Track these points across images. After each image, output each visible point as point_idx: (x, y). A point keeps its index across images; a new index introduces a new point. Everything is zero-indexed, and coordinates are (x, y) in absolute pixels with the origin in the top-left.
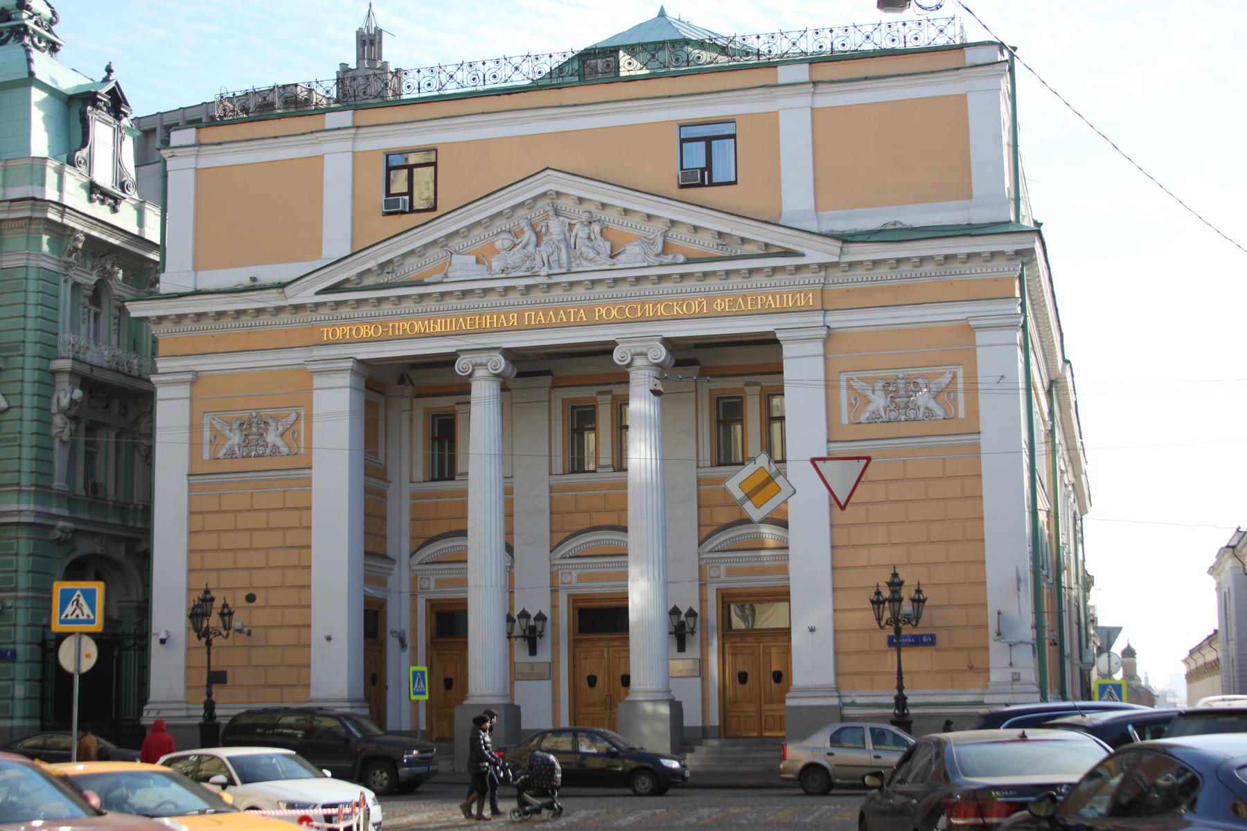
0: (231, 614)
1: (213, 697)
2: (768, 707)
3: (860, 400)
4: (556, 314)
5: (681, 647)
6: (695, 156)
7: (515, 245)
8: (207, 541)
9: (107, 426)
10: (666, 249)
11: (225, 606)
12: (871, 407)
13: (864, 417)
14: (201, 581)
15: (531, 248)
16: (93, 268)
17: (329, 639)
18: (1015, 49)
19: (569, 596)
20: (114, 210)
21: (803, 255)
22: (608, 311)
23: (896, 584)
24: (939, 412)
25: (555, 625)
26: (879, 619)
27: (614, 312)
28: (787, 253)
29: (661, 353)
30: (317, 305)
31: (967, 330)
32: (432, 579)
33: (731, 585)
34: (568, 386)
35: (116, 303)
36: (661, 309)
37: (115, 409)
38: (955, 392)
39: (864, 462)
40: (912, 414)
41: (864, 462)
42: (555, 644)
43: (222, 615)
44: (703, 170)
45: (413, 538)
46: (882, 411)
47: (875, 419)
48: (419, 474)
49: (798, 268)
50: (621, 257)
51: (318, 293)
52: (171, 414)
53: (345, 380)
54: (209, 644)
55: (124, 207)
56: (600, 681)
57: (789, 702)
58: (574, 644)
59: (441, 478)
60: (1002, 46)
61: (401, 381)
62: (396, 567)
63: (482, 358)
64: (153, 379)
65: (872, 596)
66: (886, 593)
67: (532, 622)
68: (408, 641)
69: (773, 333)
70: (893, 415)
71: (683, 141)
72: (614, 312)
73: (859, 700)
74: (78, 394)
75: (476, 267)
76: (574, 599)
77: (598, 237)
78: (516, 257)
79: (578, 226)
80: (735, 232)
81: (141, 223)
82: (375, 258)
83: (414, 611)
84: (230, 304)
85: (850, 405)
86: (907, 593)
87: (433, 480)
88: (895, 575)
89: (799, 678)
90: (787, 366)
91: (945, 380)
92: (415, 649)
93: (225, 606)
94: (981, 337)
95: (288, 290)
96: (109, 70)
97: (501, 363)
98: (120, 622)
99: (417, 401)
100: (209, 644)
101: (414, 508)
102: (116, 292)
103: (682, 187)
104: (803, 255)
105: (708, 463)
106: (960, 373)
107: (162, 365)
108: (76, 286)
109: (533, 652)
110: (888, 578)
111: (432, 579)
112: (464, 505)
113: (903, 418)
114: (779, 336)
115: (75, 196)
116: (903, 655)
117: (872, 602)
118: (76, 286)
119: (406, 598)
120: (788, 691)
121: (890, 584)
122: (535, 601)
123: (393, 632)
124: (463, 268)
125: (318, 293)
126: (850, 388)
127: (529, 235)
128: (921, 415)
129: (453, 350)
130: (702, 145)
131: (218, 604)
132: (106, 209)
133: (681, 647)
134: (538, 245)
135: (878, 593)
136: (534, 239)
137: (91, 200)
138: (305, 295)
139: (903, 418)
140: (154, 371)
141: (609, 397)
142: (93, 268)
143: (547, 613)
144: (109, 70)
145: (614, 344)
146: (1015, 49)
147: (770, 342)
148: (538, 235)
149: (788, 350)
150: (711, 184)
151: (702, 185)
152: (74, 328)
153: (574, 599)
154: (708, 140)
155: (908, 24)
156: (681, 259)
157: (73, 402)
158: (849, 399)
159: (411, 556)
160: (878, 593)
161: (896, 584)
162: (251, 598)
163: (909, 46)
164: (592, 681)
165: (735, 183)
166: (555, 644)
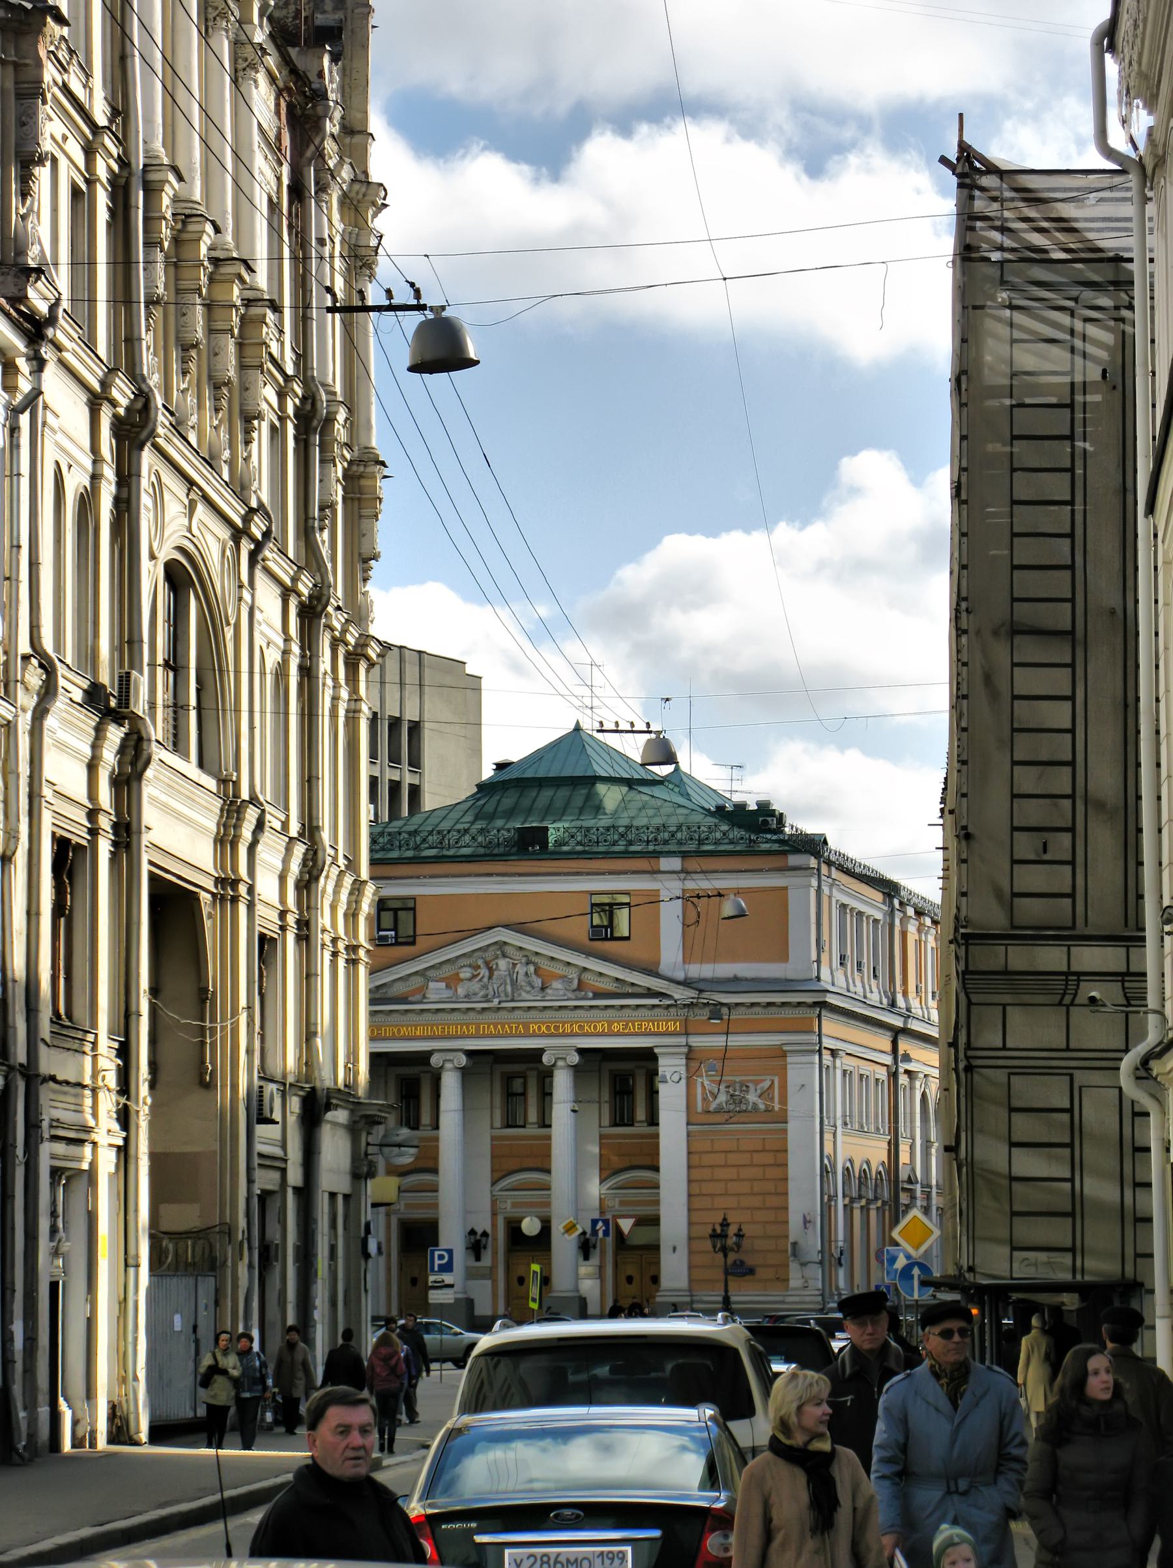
4: (503, 1028)
5: (586, 1258)
7: (474, 976)
10: (581, 986)
13: (712, 1107)
15: (486, 980)
22: (539, 1028)
23: (725, 1224)
25: (495, 1239)
26: (714, 1247)
27: (543, 1028)
29: (575, 1059)
34: (512, 1078)
36: (576, 1028)
40: (744, 1107)
42: (495, 1253)
44: (606, 927)
47: (719, 1110)
50: (549, 991)
57: (658, 1299)
63: (450, 1056)
67: (478, 1237)
69: (651, 1049)
70: (732, 1107)
72: (543, 1028)
73: (705, 1299)
78: (475, 986)
86: (732, 1230)
89: (665, 1282)
91: (767, 1084)
97: (463, 1060)
103: (591, 940)
109: (478, 1259)
114: (656, 1050)
120: (658, 1291)
121: (722, 1225)
122: (483, 1223)
127: (484, 972)
133: (586, 1258)
134: (490, 977)
135: (714, 1230)
136: (487, 973)
143: (489, 1231)
148: (491, 970)
151: (606, 939)
160: (714, 1230)
161: (725, 1224)
165: (628, 938)
166: (495, 1253)
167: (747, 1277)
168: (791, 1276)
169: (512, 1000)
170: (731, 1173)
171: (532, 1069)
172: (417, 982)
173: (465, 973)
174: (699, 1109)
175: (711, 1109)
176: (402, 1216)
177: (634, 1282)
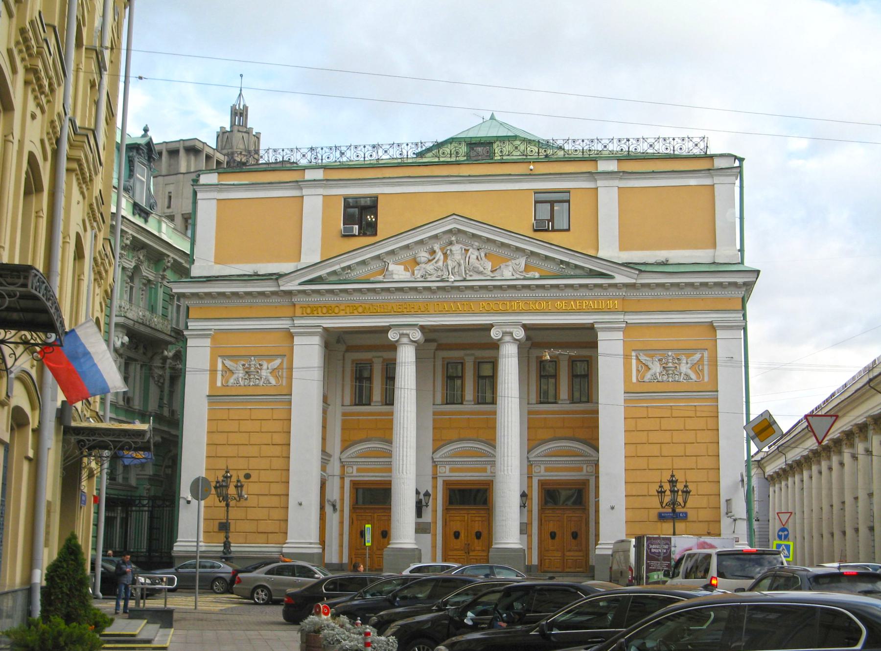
0: (242, 486)
1: (230, 540)
2: (568, 554)
6: (544, 211)
7: (430, 261)
8: (220, 438)
9: (135, 360)
11: (238, 481)
14: (222, 464)
16: (133, 257)
17: (612, 508)
18: (743, 159)
19: (444, 481)
20: (146, 221)
21: (612, 277)
24: (693, 376)
26: (661, 503)
29: (520, 334)
30: (300, 292)
31: (712, 327)
32: (355, 468)
33: (547, 478)
35: (144, 281)
37: (141, 351)
38: (703, 365)
39: (834, 418)
41: (834, 418)
42: (435, 511)
43: (236, 487)
44: (549, 221)
45: (343, 441)
48: (347, 401)
49: (610, 285)
52: (198, 355)
53: (316, 340)
54: (228, 505)
55: (151, 219)
56: (462, 535)
58: (446, 510)
59: (360, 404)
60: (736, 158)
61: (338, 341)
62: (332, 459)
64: (185, 333)
65: (657, 488)
66: (667, 487)
68: (338, 507)
69: (592, 324)
71: (536, 202)
74: (126, 339)
75: (404, 273)
77: (484, 258)
78: (430, 267)
79: (471, 250)
80: (571, 261)
81: (160, 231)
82: (339, 264)
83: (342, 488)
84: (241, 288)
85: (638, 371)
86: (680, 486)
87: (356, 405)
88: (672, 476)
90: (600, 344)
91: (697, 356)
92: (342, 511)
93: (238, 481)
94: (720, 334)
96: (146, 130)
98: (137, 488)
99: (348, 355)
100: (228, 505)
101: (344, 422)
102: (144, 274)
103: (535, 231)
104: (612, 277)
105: (534, 401)
106: (706, 354)
107: (191, 325)
108: (124, 268)
110: (669, 478)
111: (355, 468)
113: (670, 380)
115: (126, 210)
116: (677, 525)
117: (658, 492)
118: (124, 268)
119: (337, 480)
123: (329, 501)
124: (398, 272)
126: (637, 358)
127: (439, 255)
130: (548, 206)
131: (234, 479)
132: (143, 220)
136: (442, 257)
137: (134, 214)
138: (292, 285)
139: (670, 380)
140: (187, 328)
141: (473, 358)
142: (133, 257)
144: (146, 130)
145: (492, 326)
146: (743, 159)
147: (591, 329)
149: (601, 336)
150: (553, 230)
152: (121, 298)
154: (552, 203)
155: (676, 139)
156: (537, 275)
157: (123, 344)
158: (637, 367)
159: (341, 453)
162: (247, 476)
163: (676, 153)
164: (457, 535)
165: (568, 230)
166: (435, 511)
169: (465, 280)
170: (665, 437)
172: (376, 266)
173: (423, 255)
174: (634, 380)
175: (646, 379)
177: (557, 538)
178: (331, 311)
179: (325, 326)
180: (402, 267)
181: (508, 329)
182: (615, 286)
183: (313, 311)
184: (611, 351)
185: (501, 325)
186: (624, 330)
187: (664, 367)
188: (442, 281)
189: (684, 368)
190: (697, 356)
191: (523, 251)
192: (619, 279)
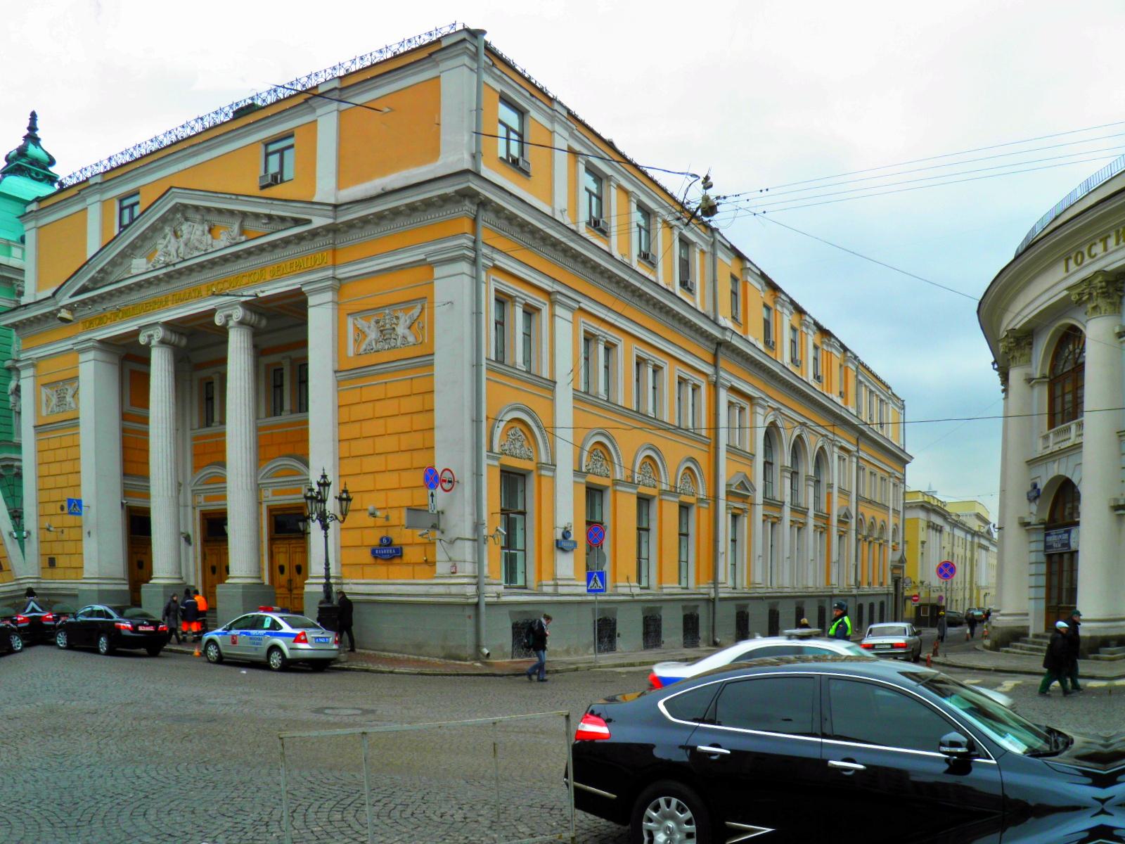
3: (360, 334)
12: (367, 341)
13: (361, 350)
21: (308, 222)
24: (411, 339)
28: (297, 222)
40: (393, 343)
46: (374, 344)
51: (70, 297)
69: (300, 288)
70: (380, 346)
76: (271, 510)
91: (416, 312)
95: (58, 296)
104: (308, 222)
112: (224, 443)
124: (139, 266)
125: (70, 297)
128: (399, 344)
129: (136, 328)
153: (271, 510)
164: (282, 569)
167: (396, 561)
168: (438, 558)
169: (184, 260)
171: (284, 358)
174: (351, 353)
176: (203, 509)
178: (101, 321)
179: (98, 338)
180: (144, 260)
181: (229, 312)
182: (314, 234)
183: (90, 324)
184: (321, 321)
185: (222, 307)
186: (332, 288)
187: (381, 331)
188: (167, 265)
189: (401, 330)
190: (416, 312)
191: (232, 213)
192: (318, 222)
